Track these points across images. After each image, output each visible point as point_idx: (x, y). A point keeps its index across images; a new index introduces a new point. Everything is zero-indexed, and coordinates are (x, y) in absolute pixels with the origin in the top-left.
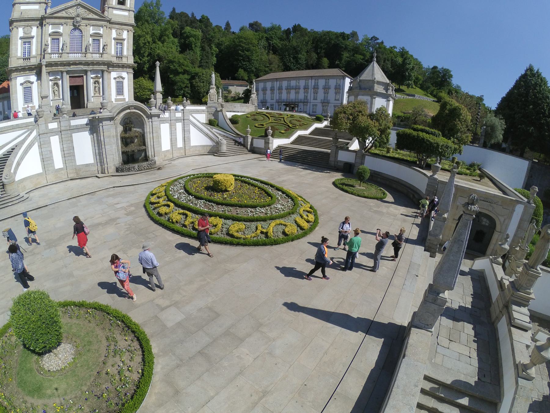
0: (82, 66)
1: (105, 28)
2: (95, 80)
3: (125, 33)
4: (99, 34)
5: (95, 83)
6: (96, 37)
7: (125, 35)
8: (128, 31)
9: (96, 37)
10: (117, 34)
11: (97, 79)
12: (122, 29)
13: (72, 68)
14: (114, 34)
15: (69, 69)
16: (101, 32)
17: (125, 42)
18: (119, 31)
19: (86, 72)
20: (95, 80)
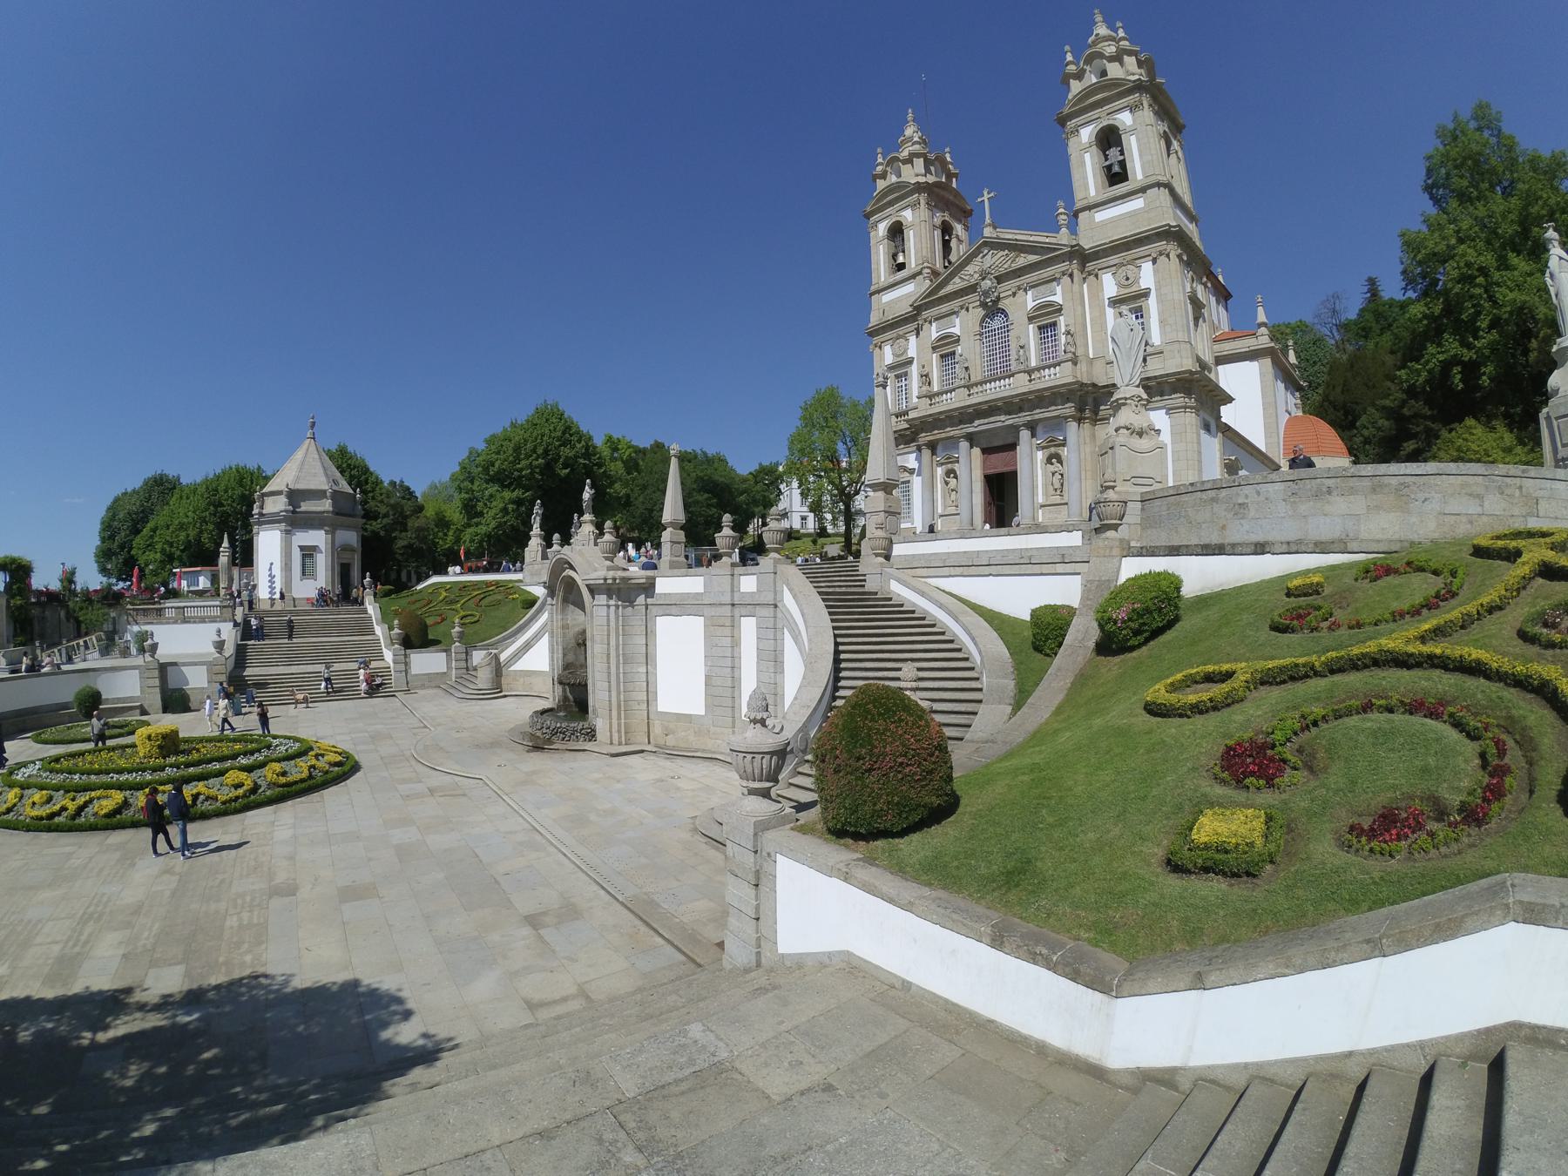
0: (1002, 418)
1: (1066, 279)
2: (1047, 452)
3: (1147, 267)
4: (1051, 304)
5: (1049, 461)
6: (1045, 320)
7: (1147, 276)
8: (1154, 261)
9: (1045, 320)
10: (1119, 285)
11: (1053, 450)
12: (1132, 262)
13: (978, 425)
14: (1110, 285)
15: (972, 430)
16: (1058, 298)
17: (1152, 303)
18: (1122, 272)
19: (1015, 429)
20: (1047, 452)
